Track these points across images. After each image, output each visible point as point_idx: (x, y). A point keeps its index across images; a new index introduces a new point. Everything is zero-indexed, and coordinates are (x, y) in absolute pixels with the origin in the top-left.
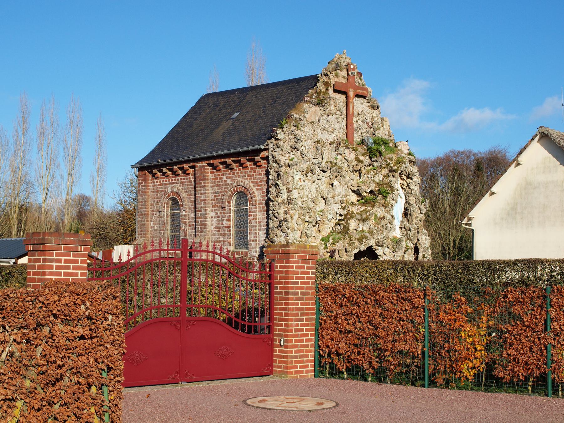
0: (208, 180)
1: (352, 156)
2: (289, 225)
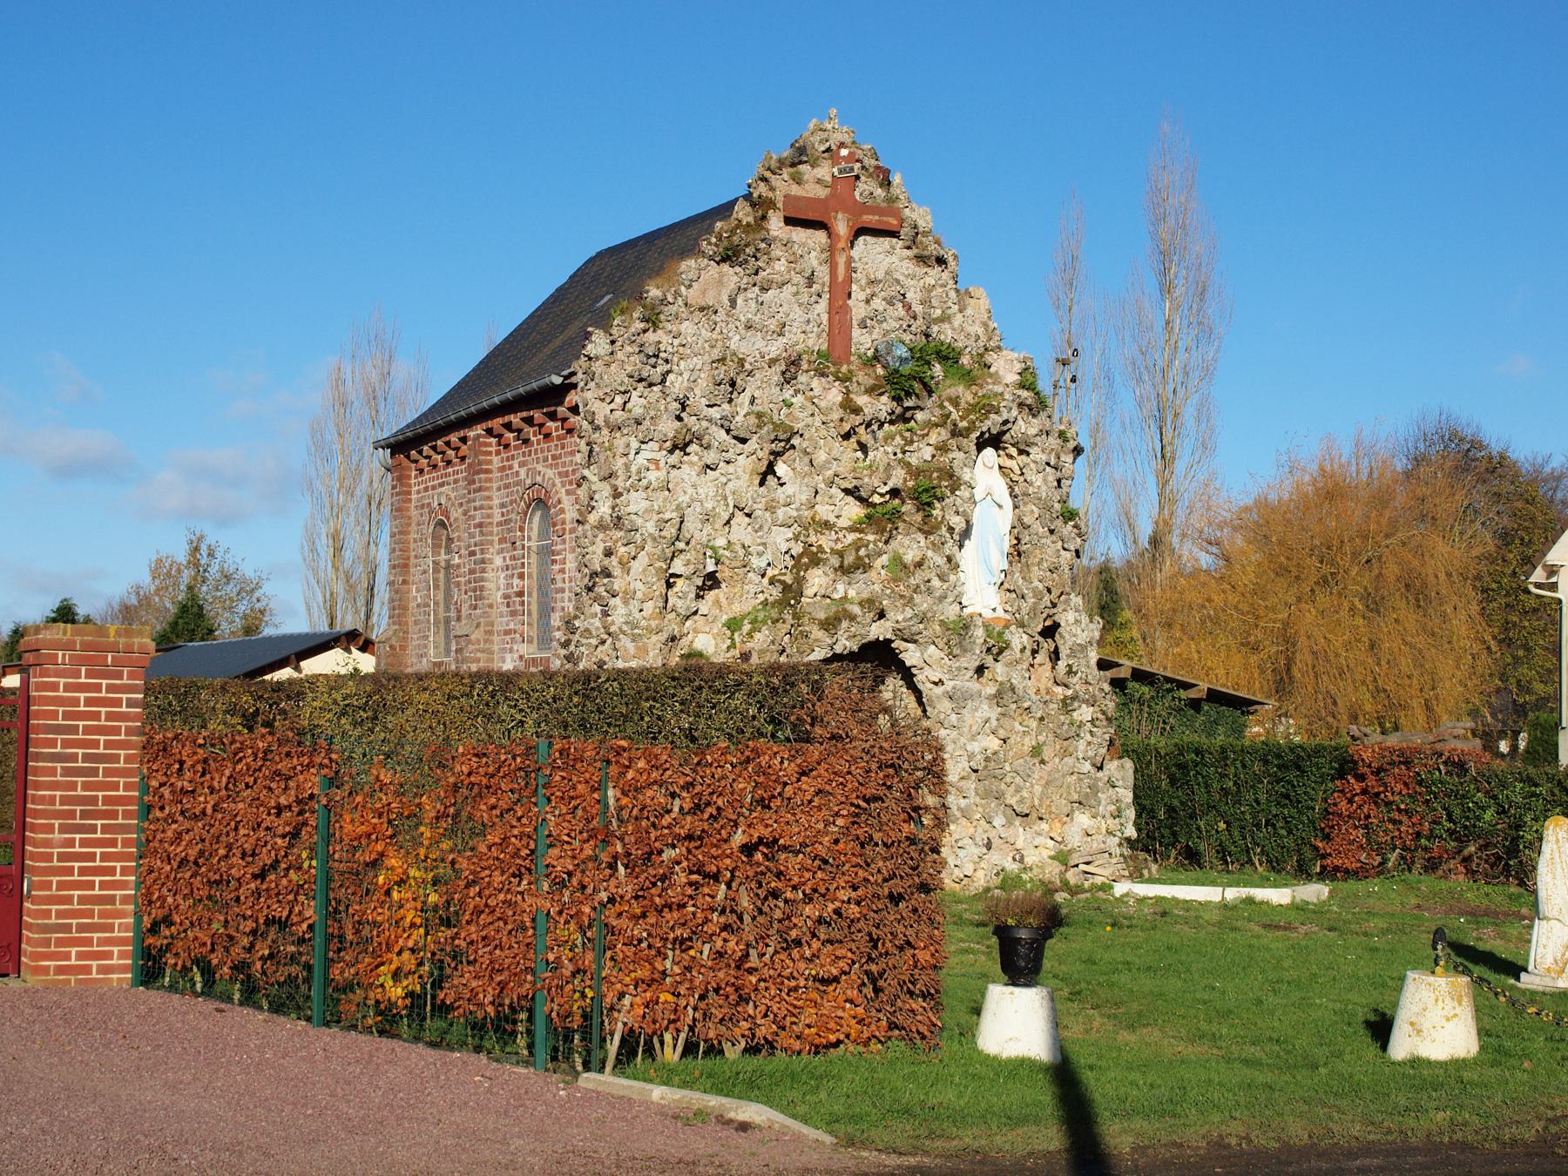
0: (488, 471)
1: (835, 395)
2: (617, 585)
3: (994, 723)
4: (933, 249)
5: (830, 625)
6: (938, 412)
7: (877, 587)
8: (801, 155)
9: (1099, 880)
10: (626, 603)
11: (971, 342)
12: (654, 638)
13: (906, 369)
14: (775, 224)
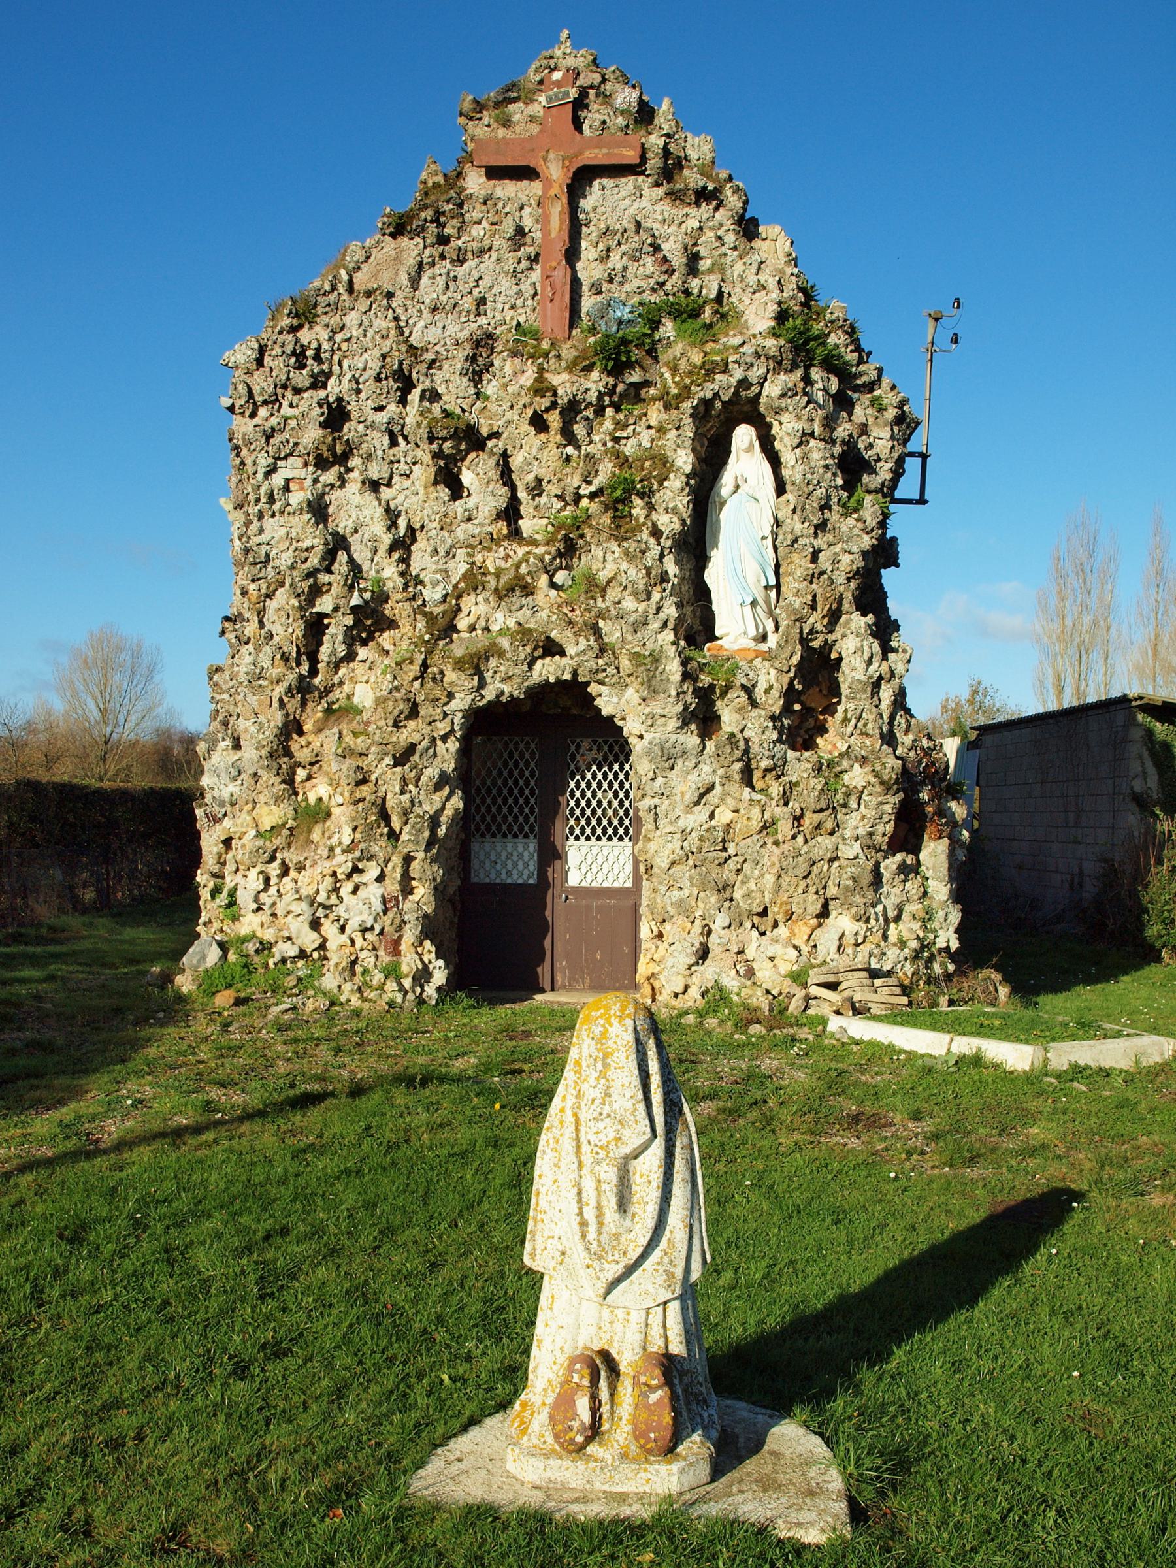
1: (528, 378)
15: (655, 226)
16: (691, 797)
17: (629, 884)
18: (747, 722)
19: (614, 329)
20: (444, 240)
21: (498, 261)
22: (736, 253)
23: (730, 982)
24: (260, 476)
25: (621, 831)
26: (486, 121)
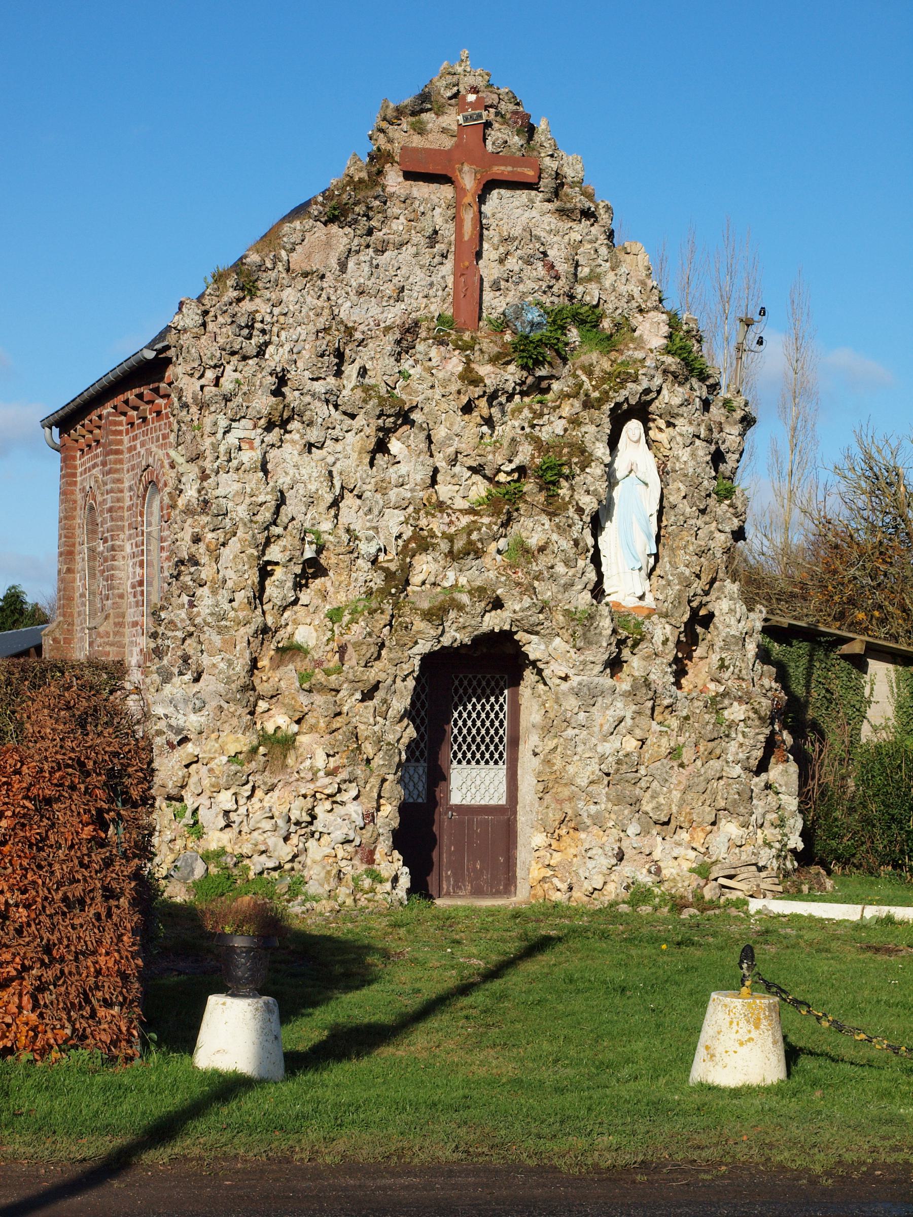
0: (118, 452)
1: (456, 364)
2: (206, 573)
3: (628, 722)
4: (579, 201)
5: (434, 617)
6: (571, 381)
7: (492, 574)
8: (425, 102)
9: (733, 896)
10: (214, 592)
11: (623, 303)
12: (243, 630)
13: (535, 336)
14: (393, 180)
15: (543, 234)
16: (607, 728)
17: (503, 802)
18: (648, 665)
19: (528, 330)
20: (370, 232)
21: (416, 255)
22: (608, 264)
23: (644, 878)
24: (219, 435)
25: (496, 756)
26: (405, 126)
